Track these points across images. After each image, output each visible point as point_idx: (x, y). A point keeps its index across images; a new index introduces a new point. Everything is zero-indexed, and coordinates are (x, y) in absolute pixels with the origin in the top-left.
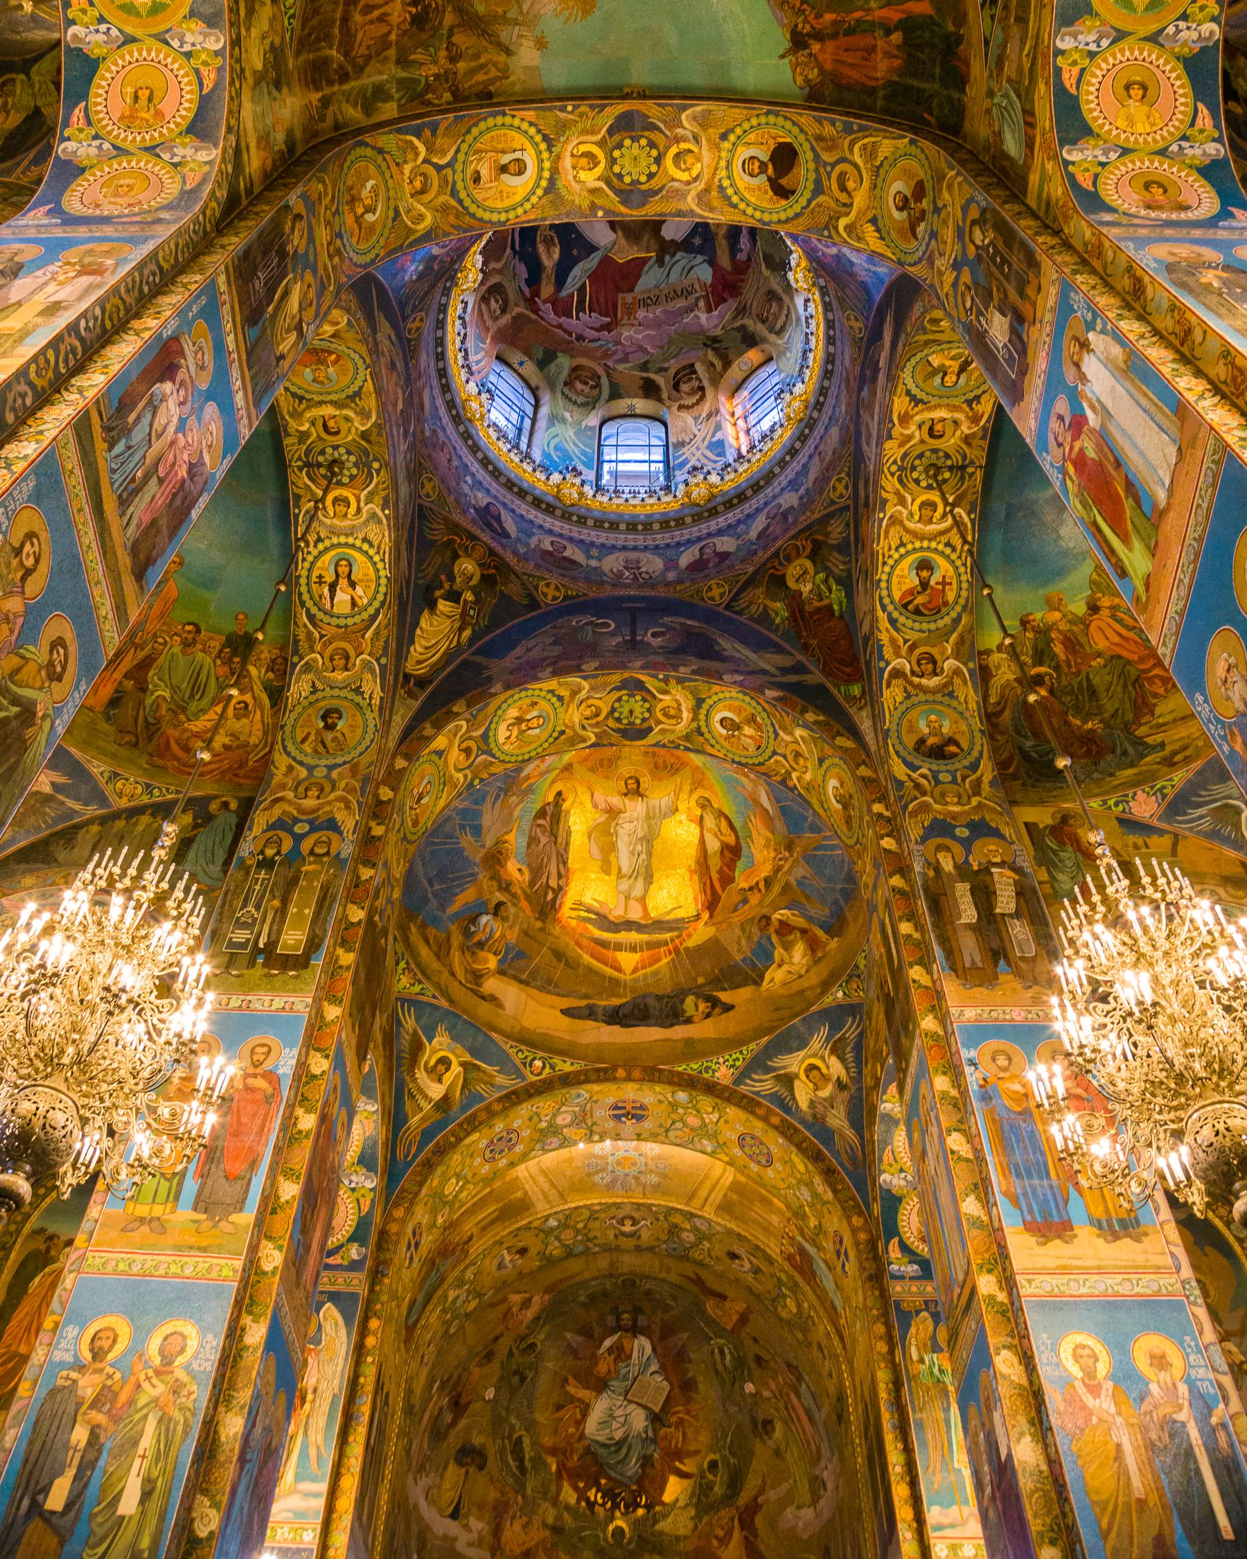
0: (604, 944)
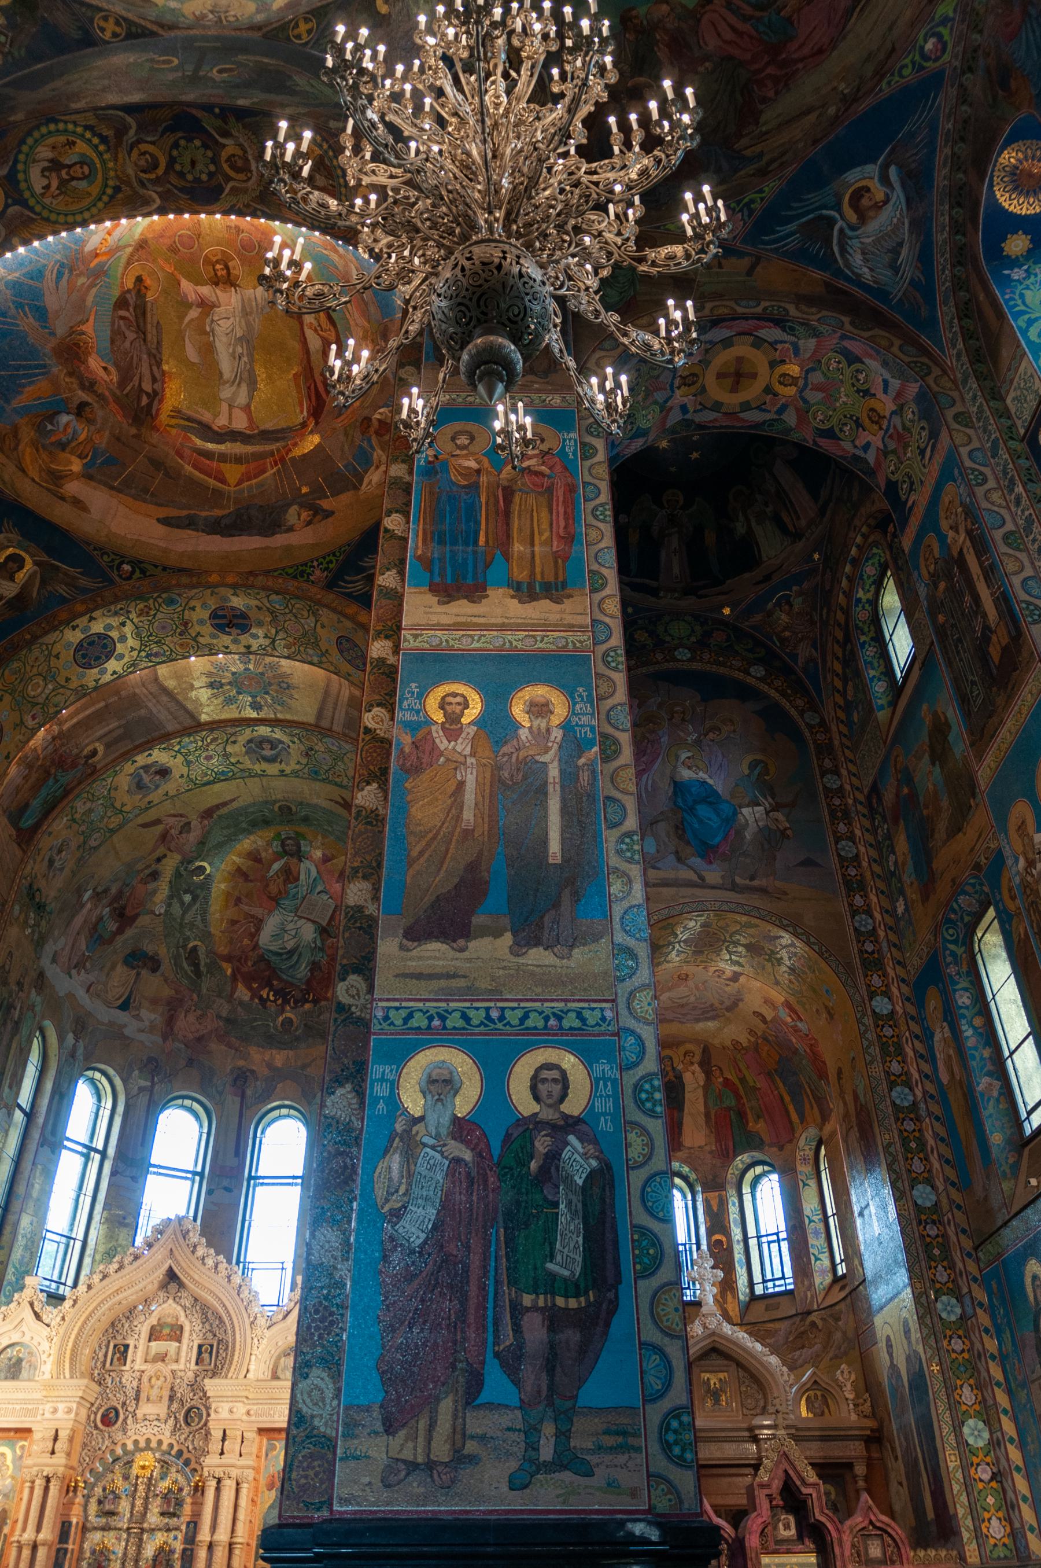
0: (208, 455)
